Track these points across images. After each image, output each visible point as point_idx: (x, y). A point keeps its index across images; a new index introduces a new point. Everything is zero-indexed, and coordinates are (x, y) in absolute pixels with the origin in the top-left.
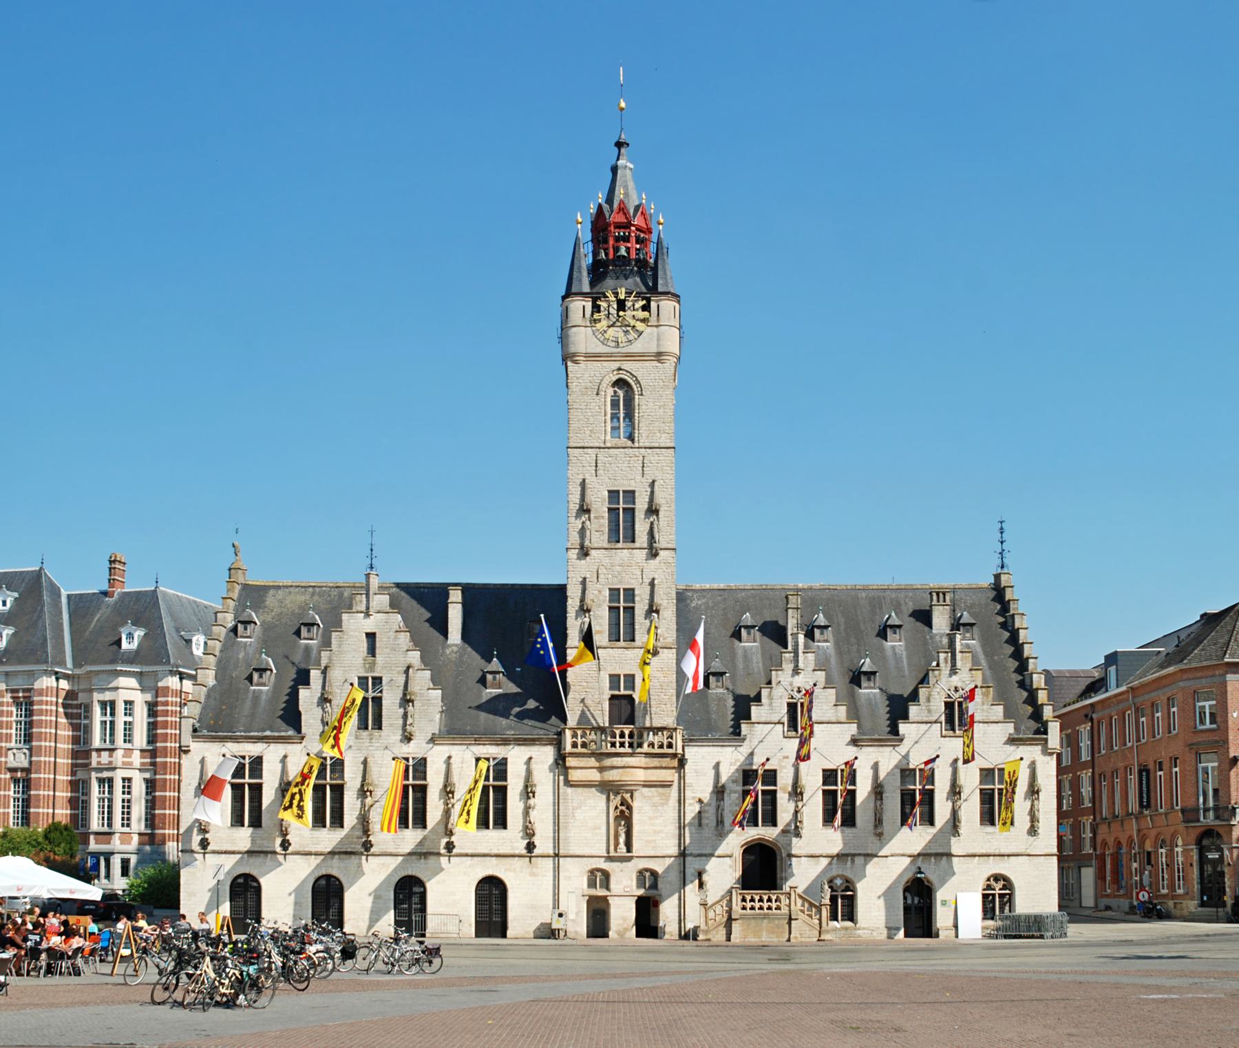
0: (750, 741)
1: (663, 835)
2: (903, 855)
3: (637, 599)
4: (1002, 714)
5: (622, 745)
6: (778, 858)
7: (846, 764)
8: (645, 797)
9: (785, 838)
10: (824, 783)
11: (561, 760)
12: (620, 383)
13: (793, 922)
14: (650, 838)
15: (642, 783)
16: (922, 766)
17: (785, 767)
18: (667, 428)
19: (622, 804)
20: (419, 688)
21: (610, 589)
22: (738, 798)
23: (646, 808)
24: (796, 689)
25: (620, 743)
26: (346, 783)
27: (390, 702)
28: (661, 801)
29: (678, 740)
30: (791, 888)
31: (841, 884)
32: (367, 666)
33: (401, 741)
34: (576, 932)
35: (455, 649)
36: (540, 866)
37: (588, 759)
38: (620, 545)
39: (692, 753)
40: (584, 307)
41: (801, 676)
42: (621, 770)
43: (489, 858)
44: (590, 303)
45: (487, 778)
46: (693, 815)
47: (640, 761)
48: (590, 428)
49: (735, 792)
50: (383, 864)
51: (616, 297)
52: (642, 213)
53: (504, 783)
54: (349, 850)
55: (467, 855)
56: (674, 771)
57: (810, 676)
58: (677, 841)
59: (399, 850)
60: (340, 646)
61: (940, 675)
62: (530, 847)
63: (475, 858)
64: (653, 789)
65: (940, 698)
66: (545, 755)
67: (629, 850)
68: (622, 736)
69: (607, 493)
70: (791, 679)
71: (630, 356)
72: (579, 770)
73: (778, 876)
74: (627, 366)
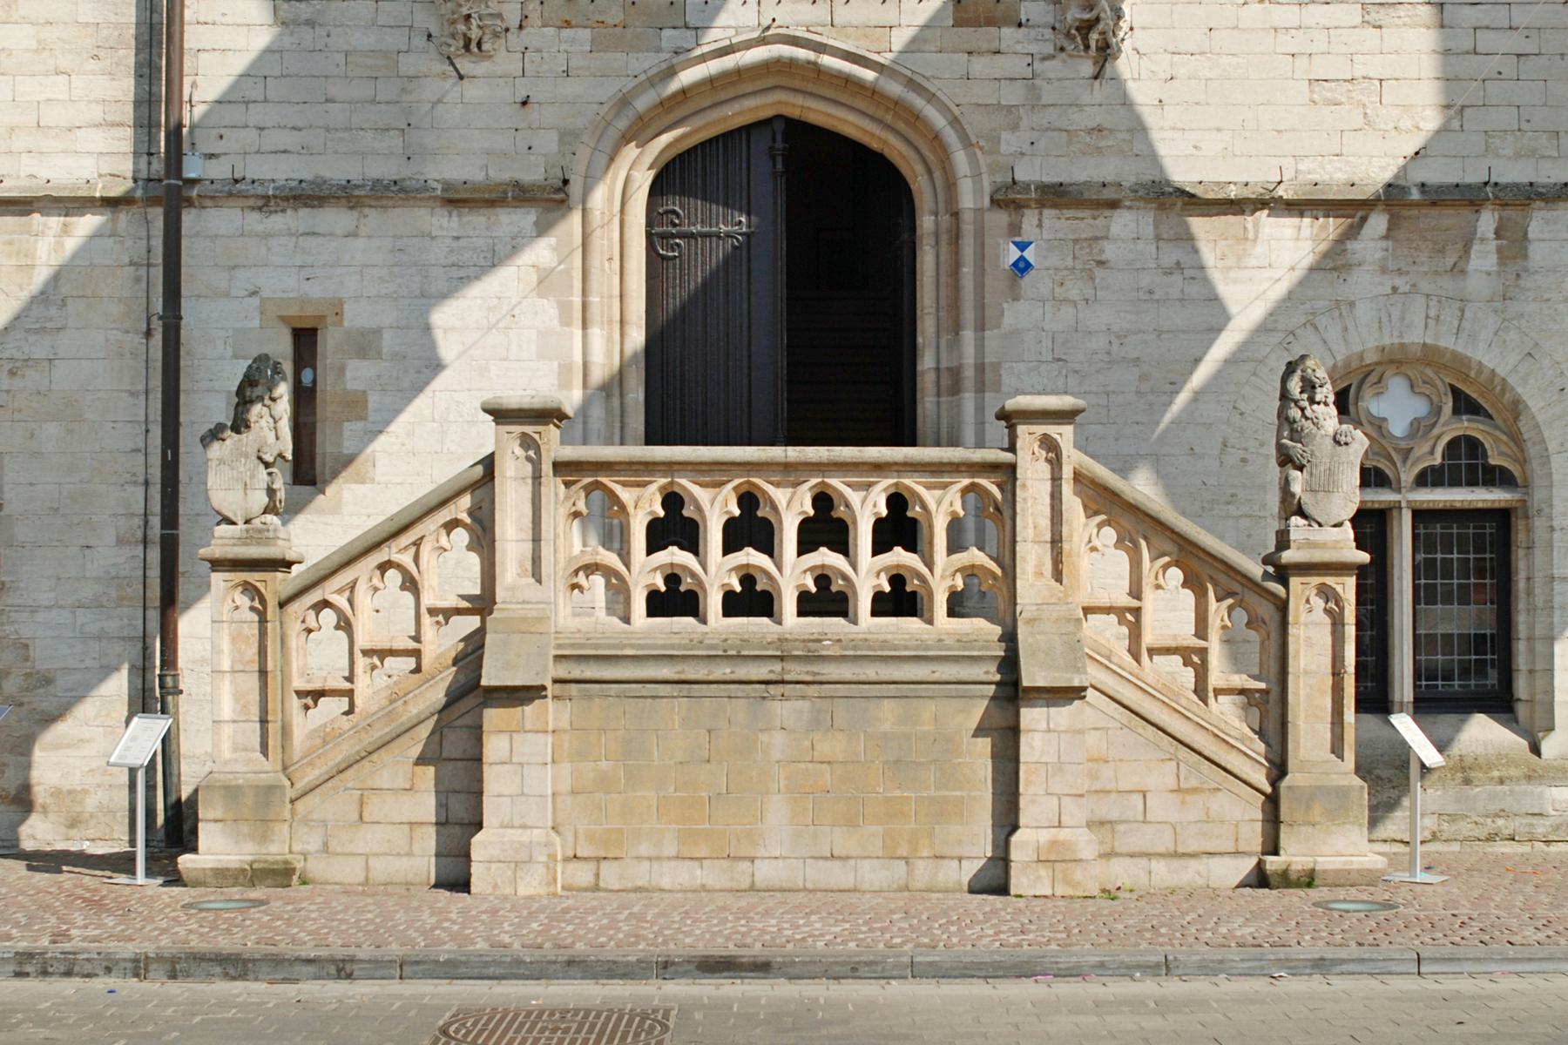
9: (980, 66)
13: (1031, 717)
31: (1419, 429)
58: (125, 87)
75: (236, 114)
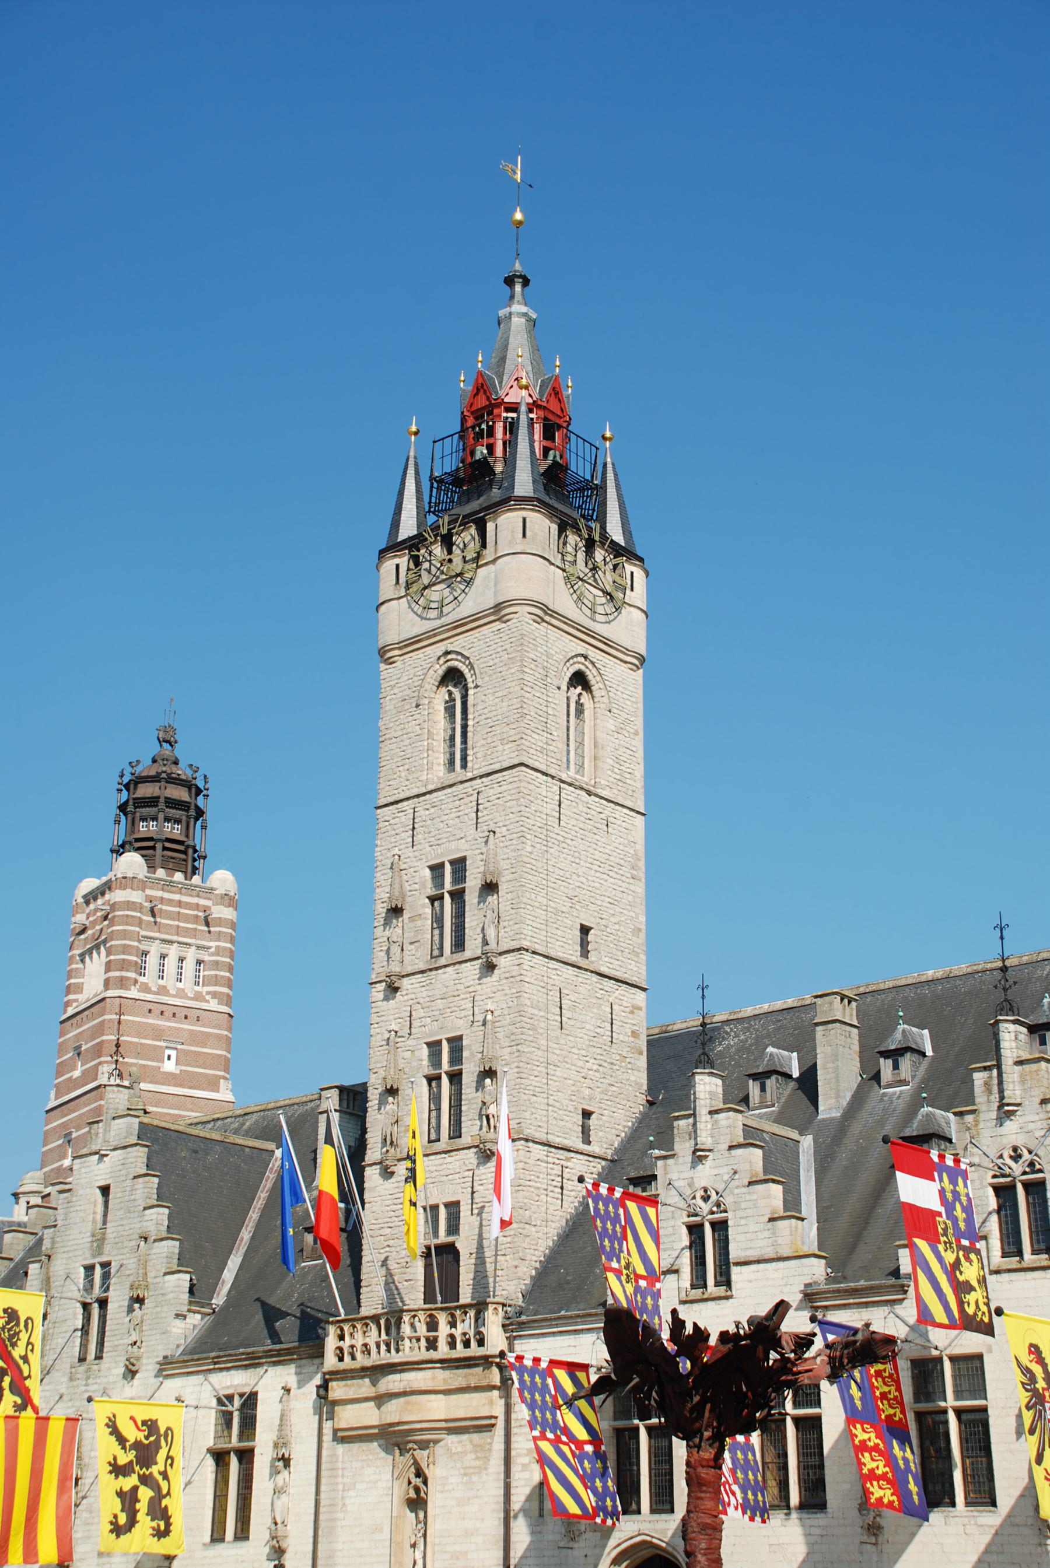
12: (452, 677)
15: (443, 1425)
18: (513, 732)
21: (428, 1044)
28: (477, 1463)
32: (95, 1245)
33: (125, 1377)
37: (360, 1381)
38: (442, 961)
40: (397, 566)
41: (708, 1163)
42: (402, 1400)
46: (527, 1491)
47: (434, 1378)
48: (406, 767)
53: (251, 1444)
56: (496, 1393)
64: (465, 1437)
69: (428, 872)
70: (689, 1174)
71: (460, 626)
74: (457, 644)
75: (524, 1561)
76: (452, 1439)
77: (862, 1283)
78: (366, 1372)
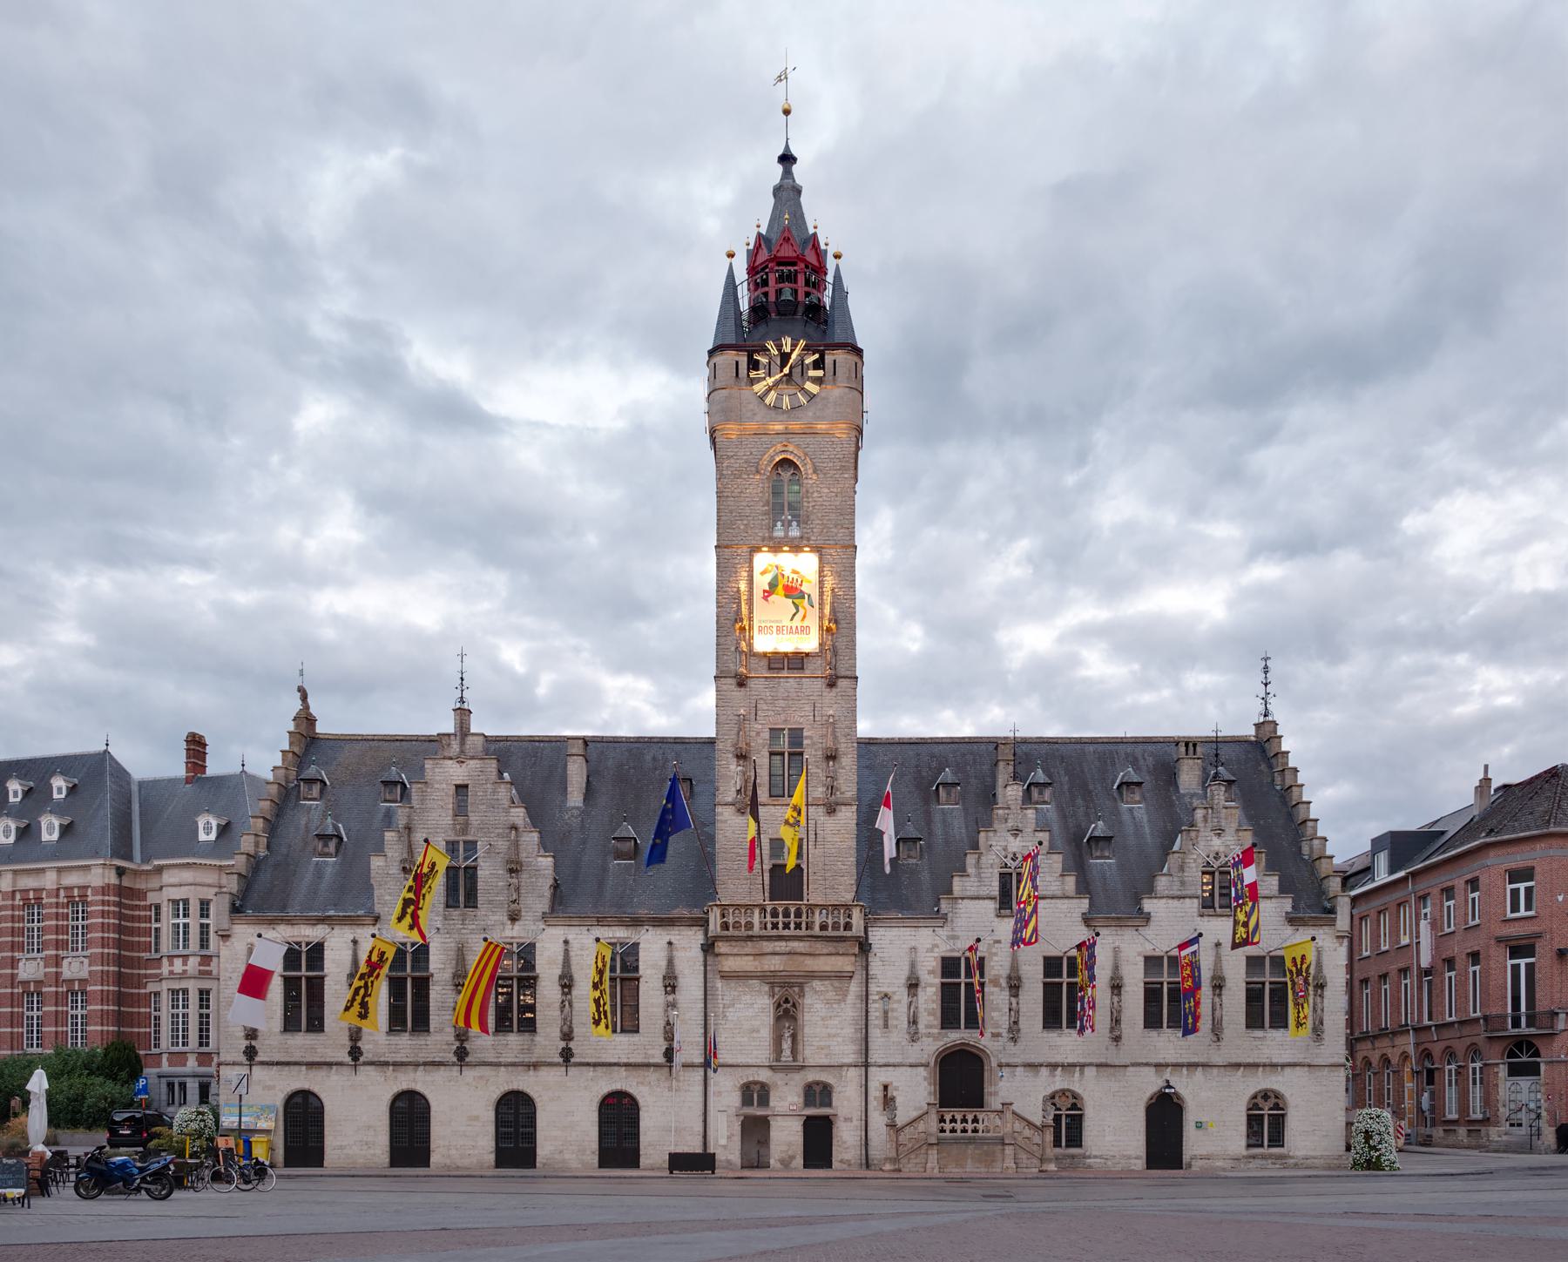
0: (952, 921)
1: (840, 1039)
2: (1147, 1064)
3: (805, 742)
4: (1276, 888)
5: (786, 926)
6: (986, 1068)
7: (1079, 947)
8: (816, 992)
10: (1046, 975)
11: (708, 948)
14: (822, 1043)
16: (1175, 952)
17: (996, 954)
19: (787, 1001)
20: (524, 855)
22: (935, 993)
23: (818, 1006)
24: (1010, 856)
25: (784, 923)
26: (432, 975)
27: (488, 872)
28: (837, 997)
29: (857, 919)
30: (1003, 1104)
32: (458, 827)
34: (728, 1161)
35: (576, 812)
36: (682, 1078)
39: (878, 936)
43: (616, 1068)
44: (746, 359)
45: (613, 969)
48: (745, 522)
49: (931, 985)
50: (481, 1077)
51: (779, 350)
52: (814, 245)
54: (437, 1059)
55: (588, 1064)
57: (1030, 839)
59: (501, 1060)
60: (422, 801)
61: (1197, 837)
62: (669, 1054)
63: (599, 1069)
65: (1197, 867)
66: (689, 942)
67: (795, 1059)
68: (786, 914)
72: (731, 958)
73: (986, 1090)
76: (817, 984)
77: (1113, 915)
78: (750, 938)
